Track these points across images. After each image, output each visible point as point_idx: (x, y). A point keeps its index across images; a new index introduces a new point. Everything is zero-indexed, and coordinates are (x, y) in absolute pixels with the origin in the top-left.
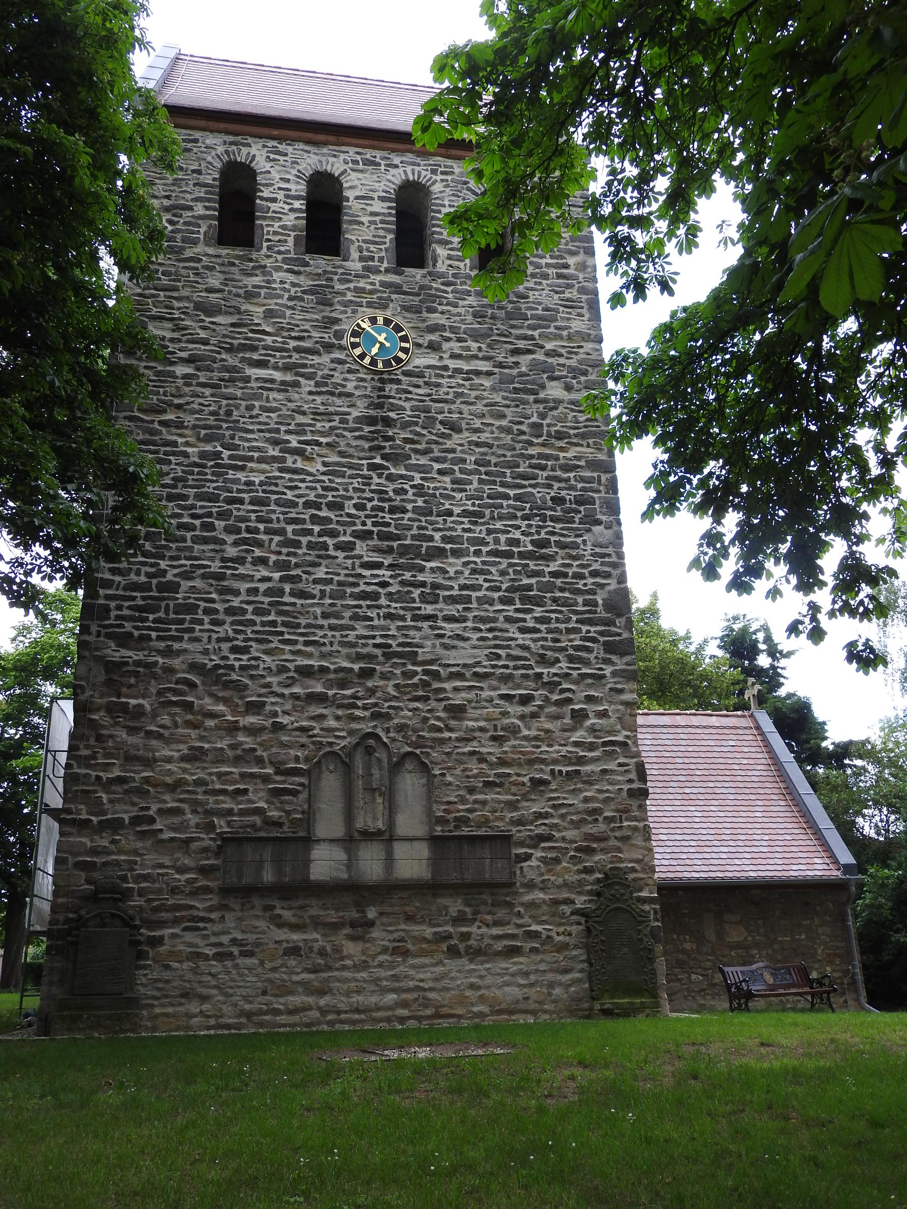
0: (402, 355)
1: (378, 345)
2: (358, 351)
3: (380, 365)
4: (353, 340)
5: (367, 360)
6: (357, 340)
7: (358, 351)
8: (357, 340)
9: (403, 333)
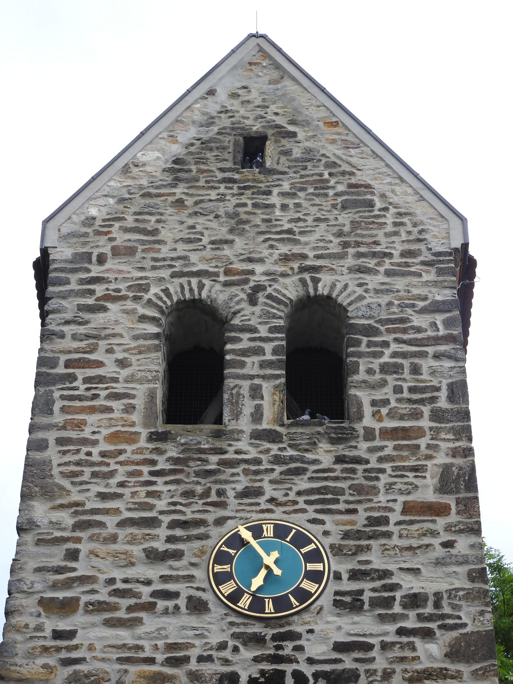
0: (308, 586)
1: (263, 572)
2: (228, 588)
3: (269, 607)
4: (218, 568)
5: (245, 601)
6: (227, 568)
7: (228, 588)
8: (227, 568)
9: (312, 546)
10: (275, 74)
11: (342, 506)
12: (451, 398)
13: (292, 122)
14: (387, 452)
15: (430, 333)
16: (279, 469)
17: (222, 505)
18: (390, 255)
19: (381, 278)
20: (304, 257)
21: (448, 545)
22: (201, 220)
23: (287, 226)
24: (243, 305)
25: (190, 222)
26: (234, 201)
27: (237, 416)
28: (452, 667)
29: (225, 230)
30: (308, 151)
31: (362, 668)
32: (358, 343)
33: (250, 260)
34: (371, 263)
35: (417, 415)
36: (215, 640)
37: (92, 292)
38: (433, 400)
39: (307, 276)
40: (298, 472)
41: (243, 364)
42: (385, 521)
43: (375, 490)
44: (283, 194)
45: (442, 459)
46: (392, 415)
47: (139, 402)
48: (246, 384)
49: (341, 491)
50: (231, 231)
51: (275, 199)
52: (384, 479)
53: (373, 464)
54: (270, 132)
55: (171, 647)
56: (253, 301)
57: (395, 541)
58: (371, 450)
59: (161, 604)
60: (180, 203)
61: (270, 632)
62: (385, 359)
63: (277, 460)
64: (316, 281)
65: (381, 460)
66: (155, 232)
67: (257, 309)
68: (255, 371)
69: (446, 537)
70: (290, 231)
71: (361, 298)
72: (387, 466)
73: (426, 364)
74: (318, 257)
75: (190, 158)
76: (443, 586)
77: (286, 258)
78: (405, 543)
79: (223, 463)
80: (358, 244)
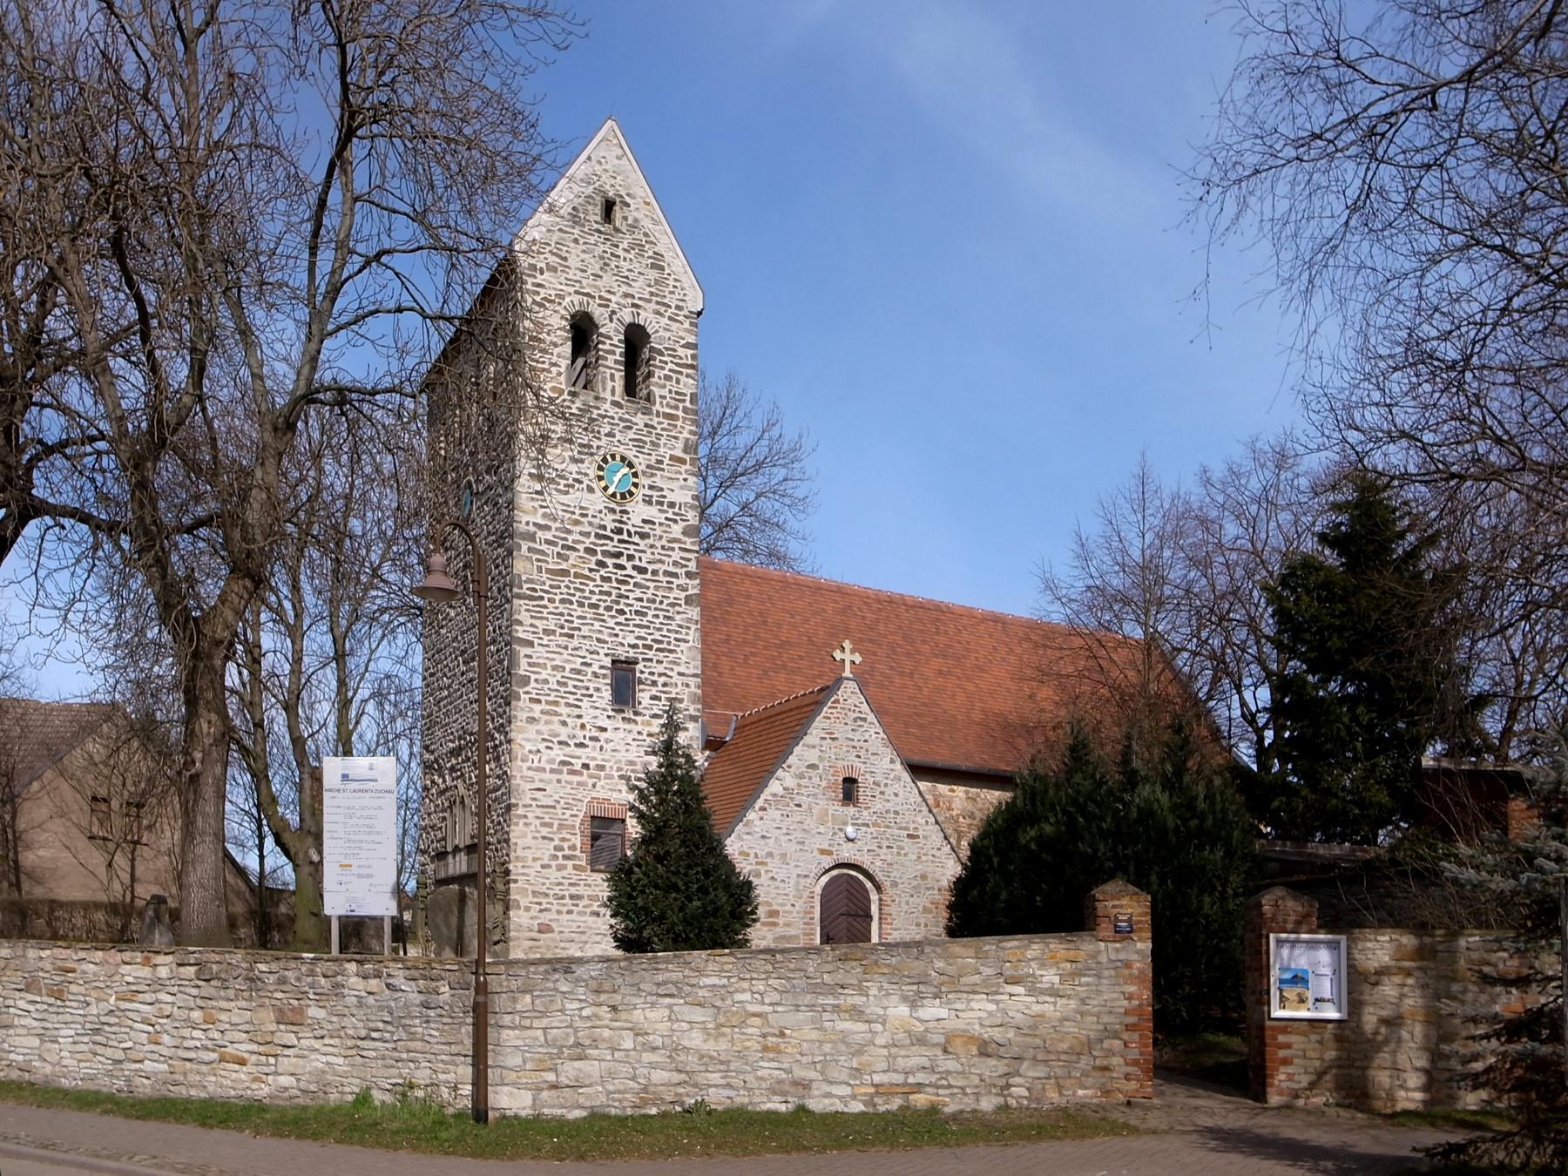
0: (633, 489)
2: (603, 484)
3: (618, 496)
7: (603, 484)
10: (620, 152)
11: (646, 451)
12: (691, 402)
13: (628, 195)
14: (665, 426)
15: (685, 361)
16: (622, 424)
17: (599, 439)
18: (670, 307)
19: (666, 320)
20: (633, 297)
21: (685, 480)
22: (586, 256)
23: (626, 274)
24: (607, 321)
25: (583, 256)
26: (602, 248)
27: (604, 389)
28: (685, 539)
29: (598, 267)
30: (636, 220)
31: (652, 533)
32: (655, 359)
33: (609, 292)
34: (662, 309)
35: (676, 408)
36: (598, 508)
37: (538, 293)
38: (684, 401)
39: (634, 310)
40: (630, 428)
41: (606, 359)
42: (661, 462)
43: (658, 445)
44: (625, 250)
45: (686, 435)
46: (668, 405)
47: (562, 370)
48: (608, 371)
49: (645, 443)
50: (601, 269)
51: (620, 252)
52: (663, 440)
53: (659, 431)
54: (618, 200)
55: (581, 508)
56: (611, 321)
57: (666, 474)
58: (659, 423)
59: (577, 485)
60: (576, 241)
61: (618, 509)
62: (666, 372)
63: (621, 419)
64: (638, 314)
65: (663, 429)
66: (565, 259)
67: (613, 325)
68: (612, 365)
69: (685, 476)
70: (627, 277)
71: (657, 331)
72: (664, 433)
73: (683, 379)
74: (640, 299)
75: (580, 208)
76: (683, 501)
77: (626, 295)
78: (670, 475)
79: (599, 415)
80: (657, 295)
